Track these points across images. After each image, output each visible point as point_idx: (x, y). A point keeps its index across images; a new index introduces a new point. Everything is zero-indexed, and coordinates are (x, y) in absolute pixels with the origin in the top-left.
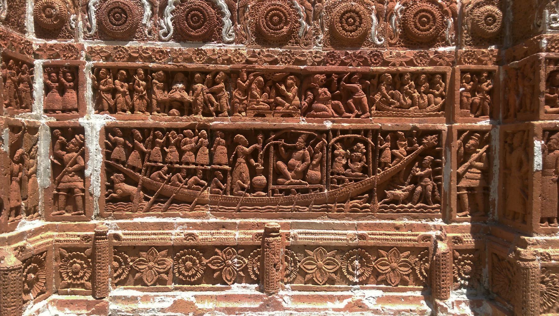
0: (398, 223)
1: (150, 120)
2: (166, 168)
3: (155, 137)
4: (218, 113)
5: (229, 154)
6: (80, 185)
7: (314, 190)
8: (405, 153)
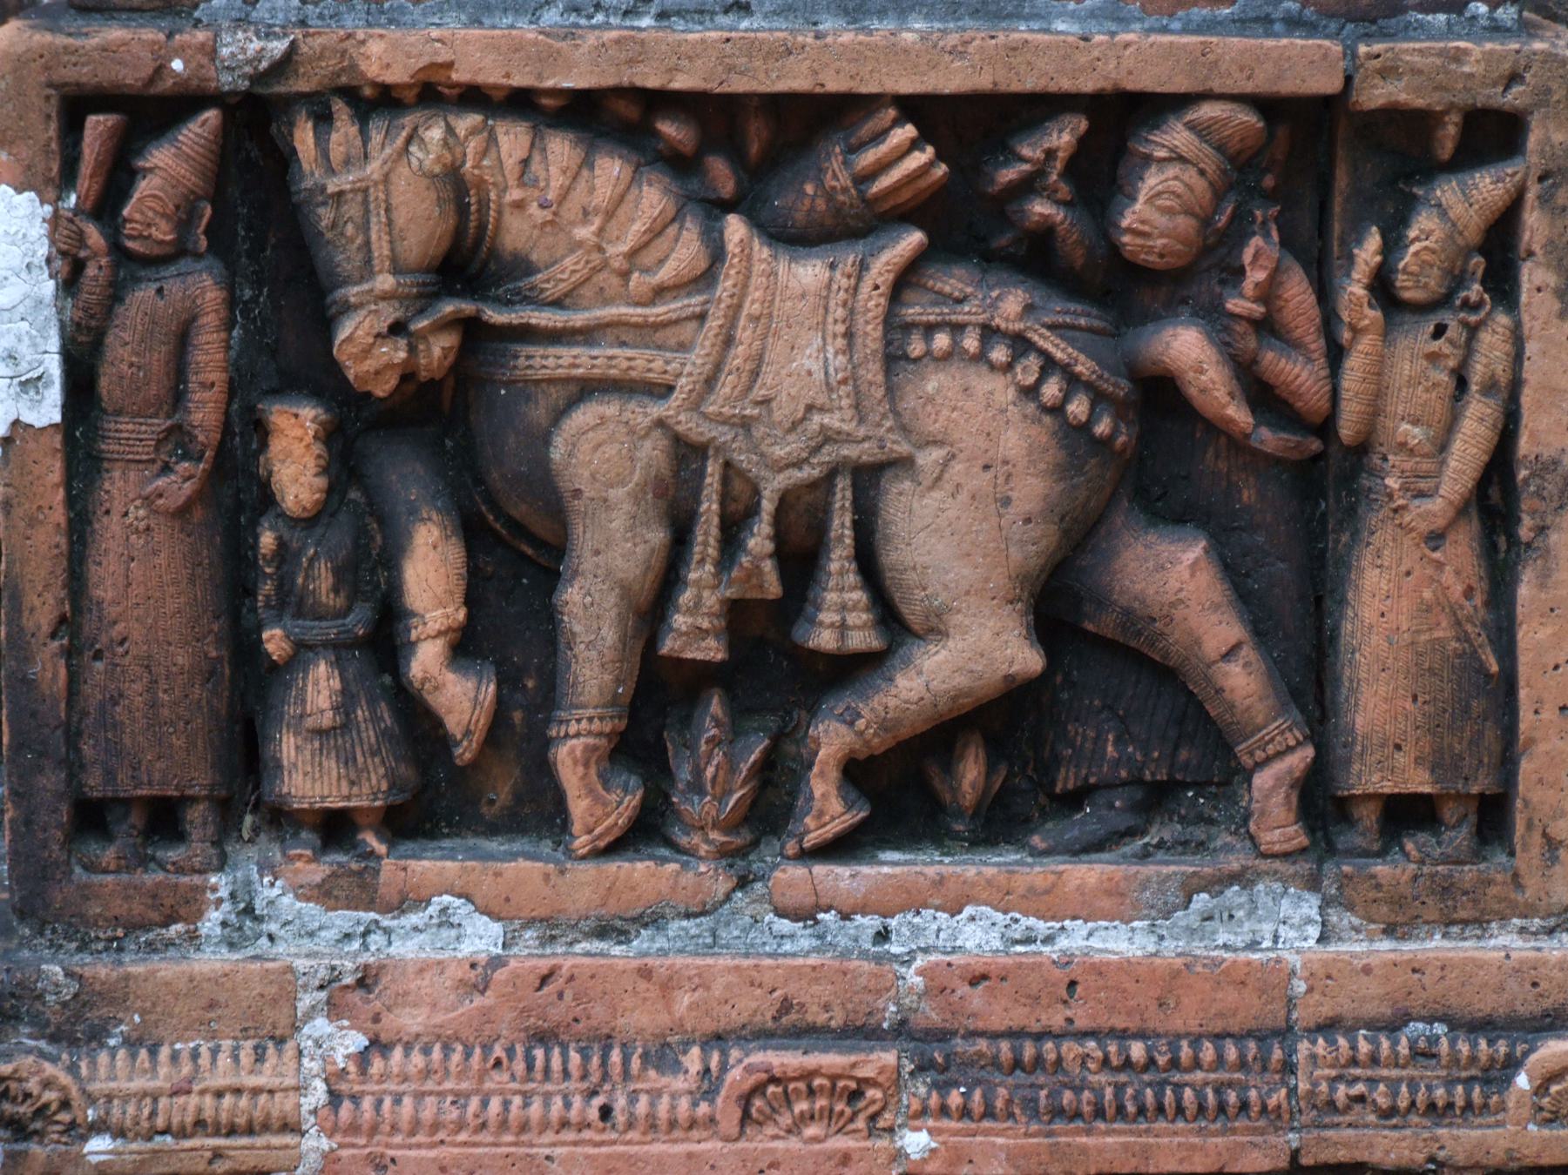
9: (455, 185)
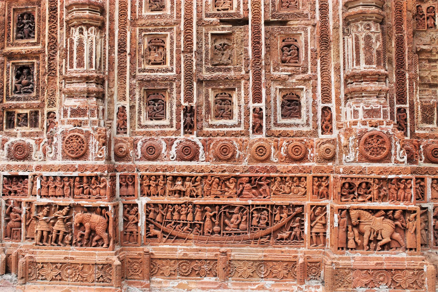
0: (283, 249)
1: (166, 200)
2: (173, 223)
3: (168, 208)
4: (197, 196)
5: (202, 216)
6: (136, 230)
7: (243, 233)
8: (287, 216)
9: (359, 214)
